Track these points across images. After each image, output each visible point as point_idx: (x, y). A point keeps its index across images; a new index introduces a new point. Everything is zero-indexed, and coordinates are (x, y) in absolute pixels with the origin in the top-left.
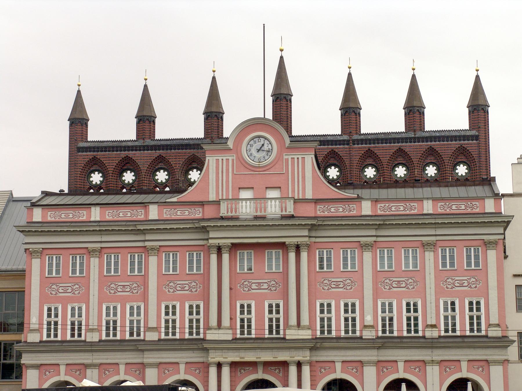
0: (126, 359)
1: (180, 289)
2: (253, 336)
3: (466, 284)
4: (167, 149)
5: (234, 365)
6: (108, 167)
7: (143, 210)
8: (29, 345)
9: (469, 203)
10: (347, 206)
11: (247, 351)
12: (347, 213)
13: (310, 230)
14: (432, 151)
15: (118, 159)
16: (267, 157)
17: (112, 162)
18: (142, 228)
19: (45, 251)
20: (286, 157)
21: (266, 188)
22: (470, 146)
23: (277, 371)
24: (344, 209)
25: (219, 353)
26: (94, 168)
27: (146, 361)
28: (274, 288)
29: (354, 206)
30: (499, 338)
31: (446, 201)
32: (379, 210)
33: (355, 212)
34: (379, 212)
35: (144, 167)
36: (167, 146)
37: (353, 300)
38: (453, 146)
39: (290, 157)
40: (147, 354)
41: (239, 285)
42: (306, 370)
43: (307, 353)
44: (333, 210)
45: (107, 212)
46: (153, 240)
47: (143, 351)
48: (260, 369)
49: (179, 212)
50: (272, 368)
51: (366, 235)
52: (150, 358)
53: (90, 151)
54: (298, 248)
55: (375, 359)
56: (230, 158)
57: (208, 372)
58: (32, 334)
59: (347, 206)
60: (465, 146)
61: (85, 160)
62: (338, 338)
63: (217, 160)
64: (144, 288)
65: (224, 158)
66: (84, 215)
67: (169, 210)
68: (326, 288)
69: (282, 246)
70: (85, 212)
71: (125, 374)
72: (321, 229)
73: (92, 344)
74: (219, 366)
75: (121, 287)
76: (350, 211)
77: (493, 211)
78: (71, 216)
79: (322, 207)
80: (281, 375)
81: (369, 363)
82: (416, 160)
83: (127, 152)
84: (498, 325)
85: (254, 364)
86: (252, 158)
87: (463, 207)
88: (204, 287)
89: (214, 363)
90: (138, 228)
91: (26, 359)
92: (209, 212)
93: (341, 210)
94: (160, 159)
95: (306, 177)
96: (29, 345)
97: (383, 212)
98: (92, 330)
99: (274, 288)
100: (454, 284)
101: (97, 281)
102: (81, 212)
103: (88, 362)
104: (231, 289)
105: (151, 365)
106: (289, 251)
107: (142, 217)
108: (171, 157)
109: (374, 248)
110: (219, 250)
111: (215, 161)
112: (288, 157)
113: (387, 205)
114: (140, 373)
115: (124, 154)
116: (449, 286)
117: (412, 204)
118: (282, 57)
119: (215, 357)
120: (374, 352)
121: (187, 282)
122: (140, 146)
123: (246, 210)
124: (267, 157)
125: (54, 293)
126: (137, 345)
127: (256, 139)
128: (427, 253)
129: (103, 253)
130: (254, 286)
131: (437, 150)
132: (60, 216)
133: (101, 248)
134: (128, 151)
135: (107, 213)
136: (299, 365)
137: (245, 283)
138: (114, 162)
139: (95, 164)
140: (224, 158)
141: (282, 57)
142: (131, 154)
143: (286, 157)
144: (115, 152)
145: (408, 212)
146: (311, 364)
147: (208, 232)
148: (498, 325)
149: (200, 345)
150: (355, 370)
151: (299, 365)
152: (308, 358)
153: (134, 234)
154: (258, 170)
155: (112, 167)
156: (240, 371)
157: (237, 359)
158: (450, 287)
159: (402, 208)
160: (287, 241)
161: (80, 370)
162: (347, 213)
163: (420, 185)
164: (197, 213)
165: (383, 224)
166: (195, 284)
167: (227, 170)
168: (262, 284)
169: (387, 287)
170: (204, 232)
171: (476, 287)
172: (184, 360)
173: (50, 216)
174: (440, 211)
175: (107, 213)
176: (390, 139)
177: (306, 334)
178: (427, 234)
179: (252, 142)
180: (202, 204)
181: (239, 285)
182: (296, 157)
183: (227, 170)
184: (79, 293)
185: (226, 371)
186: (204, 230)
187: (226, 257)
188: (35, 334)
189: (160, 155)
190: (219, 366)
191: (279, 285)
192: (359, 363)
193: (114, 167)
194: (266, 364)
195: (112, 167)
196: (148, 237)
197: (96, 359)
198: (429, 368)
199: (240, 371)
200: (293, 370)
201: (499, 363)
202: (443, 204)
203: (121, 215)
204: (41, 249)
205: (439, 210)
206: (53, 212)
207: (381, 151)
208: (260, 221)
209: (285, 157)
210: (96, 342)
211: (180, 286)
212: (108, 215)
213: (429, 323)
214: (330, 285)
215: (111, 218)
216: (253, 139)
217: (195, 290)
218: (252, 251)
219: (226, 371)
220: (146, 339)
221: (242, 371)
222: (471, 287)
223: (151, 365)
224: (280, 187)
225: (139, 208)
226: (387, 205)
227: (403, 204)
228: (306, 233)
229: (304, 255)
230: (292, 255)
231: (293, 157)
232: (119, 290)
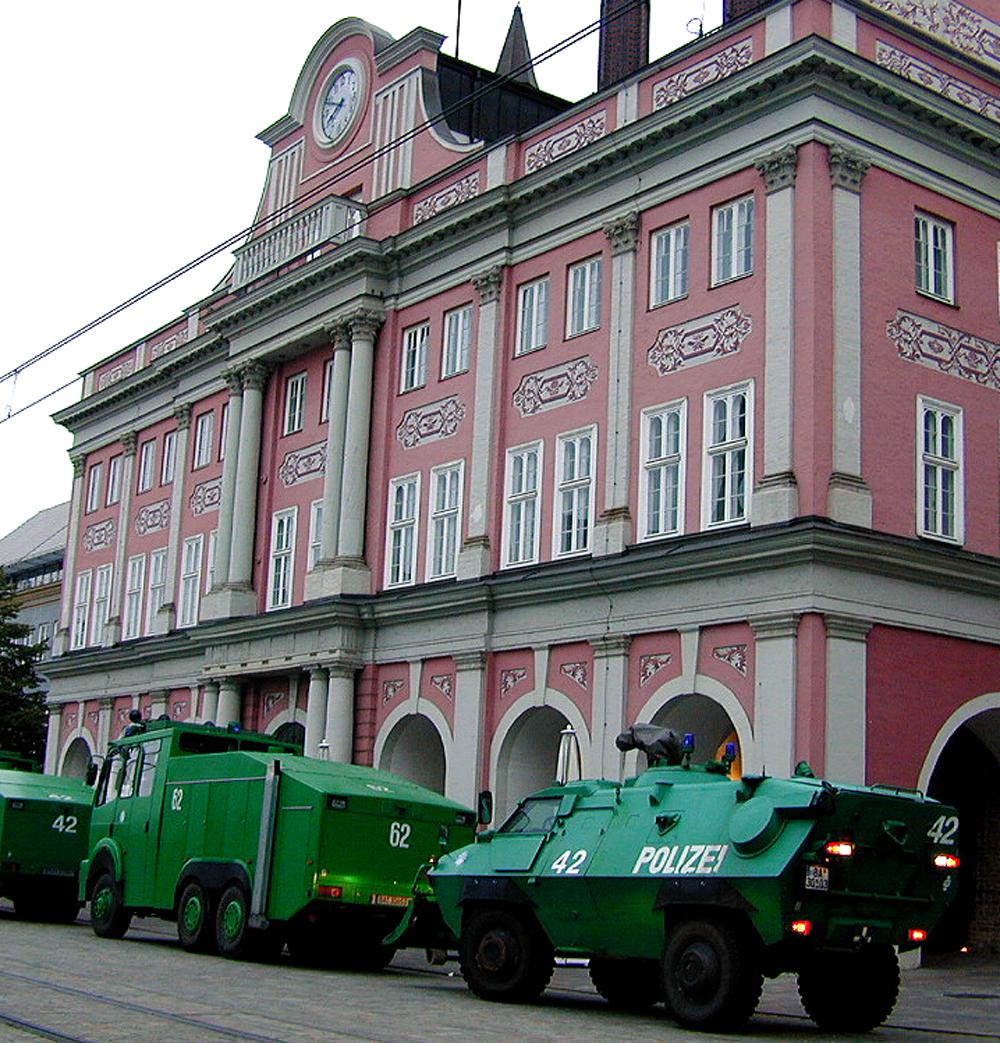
30: (782, 526)
51: (484, 254)
55: (479, 644)
89: (231, 680)
120: (479, 623)
158: (669, 363)
178: (615, 199)
201: (782, 627)
202: (663, 84)
213: (609, 507)
227: (576, 127)
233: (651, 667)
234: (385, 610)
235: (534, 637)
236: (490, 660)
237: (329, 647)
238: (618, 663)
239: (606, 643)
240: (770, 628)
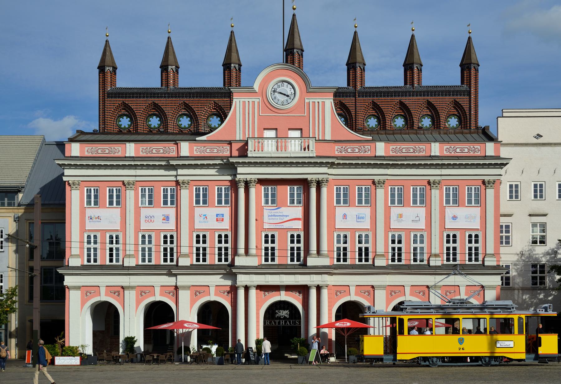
2: (276, 262)
5: (260, 288)
18: (175, 164)
34: (391, 154)
39: (311, 101)
42: (325, 293)
44: (349, 150)
49: (208, 150)
52: (183, 280)
54: (319, 184)
62: (353, 267)
63: (244, 102)
66: (119, 151)
73: (129, 268)
76: (366, 152)
77: (493, 154)
78: (107, 152)
79: (340, 147)
84: (493, 255)
86: (276, 101)
87: (466, 150)
91: (68, 281)
93: (357, 150)
98: (129, 256)
104: (256, 220)
107: (174, 154)
119: (242, 280)
123: (269, 148)
132: (97, 151)
140: (251, 100)
145: (417, 153)
147: (236, 169)
148: (493, 255)
150: (367, 293)
159: (412, 150)
160: (309, 177)
170: (231, 168)
173: (87, 151)
174: (446, 153)
175: (141, 150)
182: (316, 101)
185: (253, 293)
187: (253, 191)
194: (289, 288)
196: (180, 172)
200: (313, 293)
205: (445, 153)
209: (307, 101)
212: (142, 151)
226: (399, 147)
229: (324, 190)
230: (313, 191)
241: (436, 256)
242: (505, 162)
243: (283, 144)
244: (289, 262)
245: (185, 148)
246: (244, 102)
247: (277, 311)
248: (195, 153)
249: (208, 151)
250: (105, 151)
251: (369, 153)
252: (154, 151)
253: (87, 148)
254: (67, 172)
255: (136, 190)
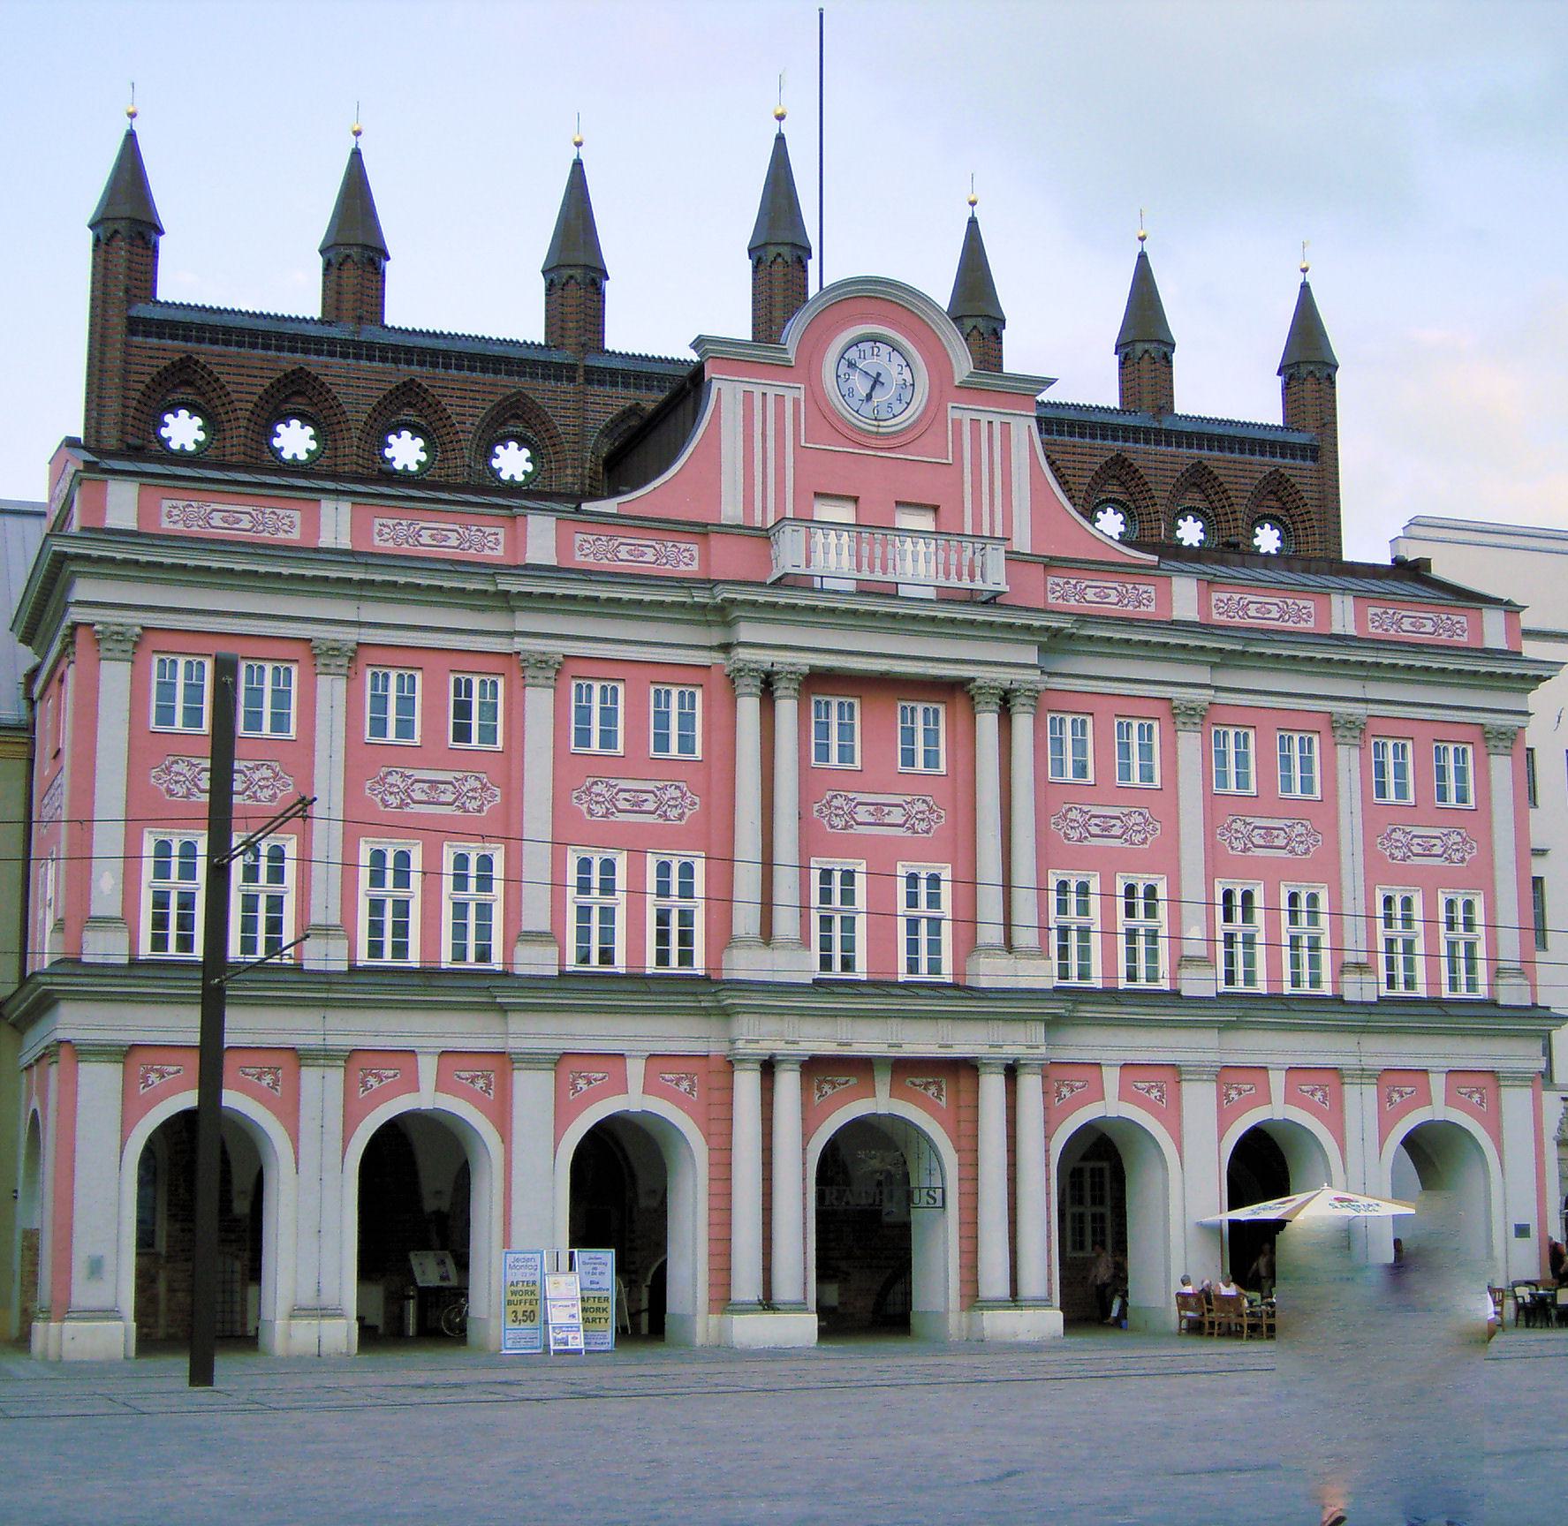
0: (442, 1035)
1: (627, 806)
3: (1437, 850)
4: (435, 365)
5: (815, 1068)
6: (234, 396)
7: (501, 531)
8: (90, 971)
9: (1444, 617)
10: (1130, 587)
11: (859, 1021)
12: (1130, 608)
13: (1043, 649)
14: (1199, 478)
15: (268, 373)
16: (897, 408)
17: (250, 380)
18: (514, 589)
19: (152, 637)
20: (957, 414)
21: (898, 503)
22: (1298, 473)
23: (933, 1089)
24: (1121, 596)
25: (770, 1025)
26: (178, 396)
27: (513, 1044)
28: (924, 825)
29: (1151, 589)
31: (1390, 604)
32: (1214, 611)
33: (1152, 609)
34: (1216, 618)
35: (358, 411)
36: (435, 352)
37: (1150, 879)
38: (1257, 468)
39: (967, 417)
40: (517, 1022)
41: (816, 807)
42: (1030, 1085)
43: (1038, 1032)
44: (1090, 595)
45: (378, 521)
46: (541, 634)
47: (503, 1009)
48: (883, 1083)
50: (917, 1081)
51: (1187, 681)
53: (173, 337)
54: (1006, 703)
56: (789, 396)
57: (731, 1088)
58: (101, 935)
59: (1130, 587)
60: (1287, 472)
61: (155, 362)
63: (748, 395)
64: (507, 796)
65: (771, 392)
66: (292, 525)
67: (591, 538)
68: (1075, 834)
69: (952, 691)
70: (297, 516)
71: (441, 1086)
72: (1078, 653)
73: (325, 978)
74: (768, 1068)
75: (426, 786)
79: (1061, 581)
80: (943, 1102)
81: (1199, 1071)
82: (1163, 494)
83: (299, 356)
85: (862, 1067)
87: (1429, 628)
88: (707, 806)
90: (501, 587)
92: (729, 559)
94: (408, 394)
95: (1014, 488)
96: (90, 971)
97: (1224, 618)
98: (326, 930)
99: (924, 825)
100: (1408, 847)
101: (339, 757)
102: (281, 512)
103: (313, 1041)
105: (533, 1060)
106: (979, 708)
108: (445, 392)
109: (1206, 724)
110: (768, 686)
111: (740, 397)
112: (959, 413)
113: (1236, 597)
114: (488, 1086)
115: (290, 360)
116: (1396, 853)
117: (1302, 603)
118: (780, 139)
121: (650, 786)
122: (345, 343)
124: (897, 408)
125: (180, 790)
126: (489, 990)
127: (866, 346)
128: (1342, 751)
129: (362, 660)
130: (862, 814)
131: (1216, 472)
132: (207, 519)
133: (358, 644)
134: (306, 351)
135: (377, 528)
136: (1012, 1072)
137: (835, 803)
138: (256, 381)
139: (182, 383)
140: (771, 392)
141: (780, 139)
142: (314, 363)
143: (957, 414)
144: (260, 351)
146: (1050, 1070)
149: (711, 995)
150: (1155, 1093)
151: (1012, 1072)
152: (1043, 1050)
153: (473, 608)
154: (873, 443)
155: (248, 397)
156: (820, 1089)
157: (829, 1049)
161: (274, 1070)
162: (1129, 610)
163: (1237, 558)
164: (685, 559)
165: (1243, 653)
166: (677, 794)
167: (780, 432)
168: (886, 809)
169: (1238, 845)
171: (1463, 860)
172: (645, 1046)
176: (1093, 425)
177: (1042, 974)
179: (852, 354)
180: (701, 531)
181: (816, 807)
182: (984, 419)
183: (780, 432)
184: (274, 796)
186: (722, 614)
187: (786, 709)
188: (110, 935)
189: (412, 380)
190: (768, 1068)
191: (939, 817)
192: (1169, 1071)
193: (256, 398)
194: (905, 1068)
195: (248, 397)
196: (524, 622)
197: (338, 1033)
198: (1351, 1092)
199: (820, 1089)
200: (992, 1086)
202: (1379, 611)
203: (425, 540)
204: (138, 630)
206: (181, 504)
207: (1067, 457)
208: (877, 606)
210: (339, 973)
211: (626, 795)
213: (1349, 957)
214: (1085, 826)
215: (390, 544)
216: (856, 343)
217: (676, 812)
218: (856, 702)
219: (788, 1083)
220: (519, 970)
221: (826, 1087)
222: (1449, 859)
223: (533, 1060)
224: (936, 509)
225: (491, 520)
228: (1030, 655)
229: (1023, 724)
230: (988, 722)
231: (975, 416)
232: (418, 796)
233: (1396, 1096)
234: (1087, 1011)
235: (1274, 1059)
236: (1226, 1075)
237: (1024, 1041)
238: (1371, 1091)
239: (1363, 1074)
240: (1515, 1079)
241: (1360, 967)
242: (1546, 674)
243: (878, 550)
244: (903, 977)
245: (542, 537)
246: (748, 395)
247: (861, 1154)
248: (579, 558)
249: (626, 553)
250: (239, 521)
251: (1152, 609)
252: (425, 540)
253: (166, 504)
254: (83, 590)
255: (352, 677)
